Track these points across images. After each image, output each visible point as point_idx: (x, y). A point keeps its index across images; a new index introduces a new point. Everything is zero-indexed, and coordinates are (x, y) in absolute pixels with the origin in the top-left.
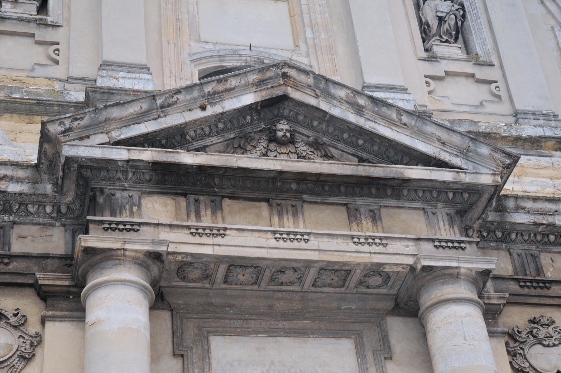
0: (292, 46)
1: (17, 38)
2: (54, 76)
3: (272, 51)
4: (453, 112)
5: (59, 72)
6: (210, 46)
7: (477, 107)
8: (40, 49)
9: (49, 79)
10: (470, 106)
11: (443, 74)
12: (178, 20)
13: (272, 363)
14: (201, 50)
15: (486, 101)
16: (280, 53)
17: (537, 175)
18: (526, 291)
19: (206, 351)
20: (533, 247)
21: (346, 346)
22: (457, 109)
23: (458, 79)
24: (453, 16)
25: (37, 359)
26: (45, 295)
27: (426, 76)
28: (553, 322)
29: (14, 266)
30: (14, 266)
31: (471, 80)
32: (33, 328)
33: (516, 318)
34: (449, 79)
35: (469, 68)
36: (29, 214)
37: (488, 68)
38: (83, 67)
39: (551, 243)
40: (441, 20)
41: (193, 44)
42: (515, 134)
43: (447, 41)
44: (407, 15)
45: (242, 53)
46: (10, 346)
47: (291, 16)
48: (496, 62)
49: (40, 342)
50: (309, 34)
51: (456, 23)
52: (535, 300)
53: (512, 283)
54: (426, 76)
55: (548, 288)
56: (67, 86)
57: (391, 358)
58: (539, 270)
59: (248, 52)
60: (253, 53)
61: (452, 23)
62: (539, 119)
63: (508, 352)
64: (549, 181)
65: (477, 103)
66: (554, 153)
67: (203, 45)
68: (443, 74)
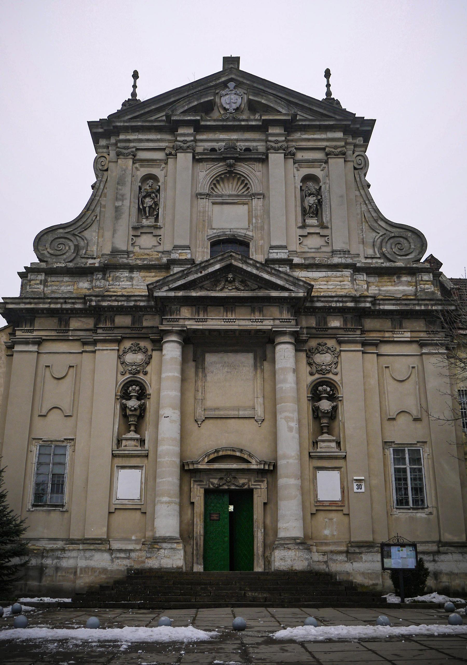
0: (247, 227)
1: (147, 235)
2: (159, 250)
3: (239, 231)
4: (308, 252)
5: (160, 249)
6: (215, 231)
7: (318, 249)
8: (155, 238)
9: (157, 252)
10: (315, 248)
11: (307, 234)
12: (204, 221)
13: (225, 362)
14: (211, 233)
15: (322, 246)
16: (242, 231)
17: (334, 281)
18: (318, 332)
19: (204, 360)
20: (325, 314)
21: (251, 355)
22: (310, 250)
23: (313, 235)
24: (315, 205)
25: (151, 363)
26: (154, 341)
27: (299, 236)
28: (326, 344)
29: (144, 331)
30: (144, 331)
31: (318, 235)
32: (149, 353)
33: (313, 343)
34: (310, 236)
35: (317, 230)
36: (148, 312)
37: (326, 229)
38: (168, 247)
39: (331, 312)
40: (310, 206)
41: (209, 231)
42: (329, 262)
43: (312, 217)
44: (296, 206)
45: (227, 233)
46: (142, 359)
47: (249, 212)
48: (330, 227)
49: (151, 358)
50: (254, 221)
51: (317, 207)
52: (321, 336)
53: (314, 329)
54: (299, 236)
55: (327, 331)
56: (163, 255)
57: (265, 360)
58: (326, 323)
59: (229, 233)
60: (232, 233)
61: (314, 208)
62: (341, 254)
63: (307, 356)
64: (339, 283)
65: (319, 247)
66: (344, 270)
67: (213, 230)
68: (307, 234)
